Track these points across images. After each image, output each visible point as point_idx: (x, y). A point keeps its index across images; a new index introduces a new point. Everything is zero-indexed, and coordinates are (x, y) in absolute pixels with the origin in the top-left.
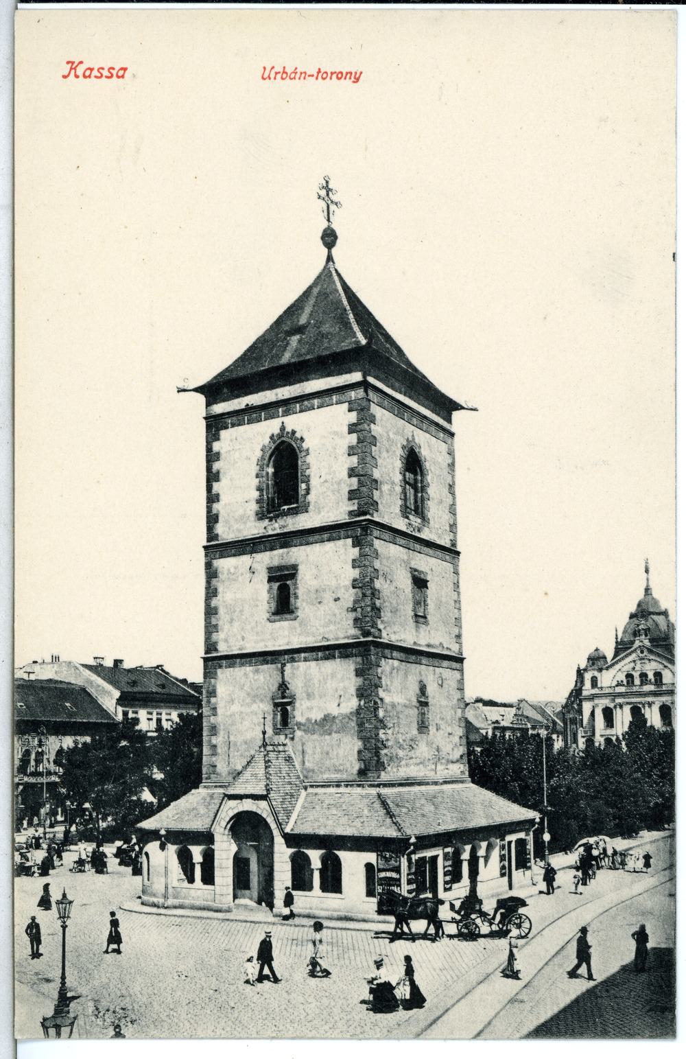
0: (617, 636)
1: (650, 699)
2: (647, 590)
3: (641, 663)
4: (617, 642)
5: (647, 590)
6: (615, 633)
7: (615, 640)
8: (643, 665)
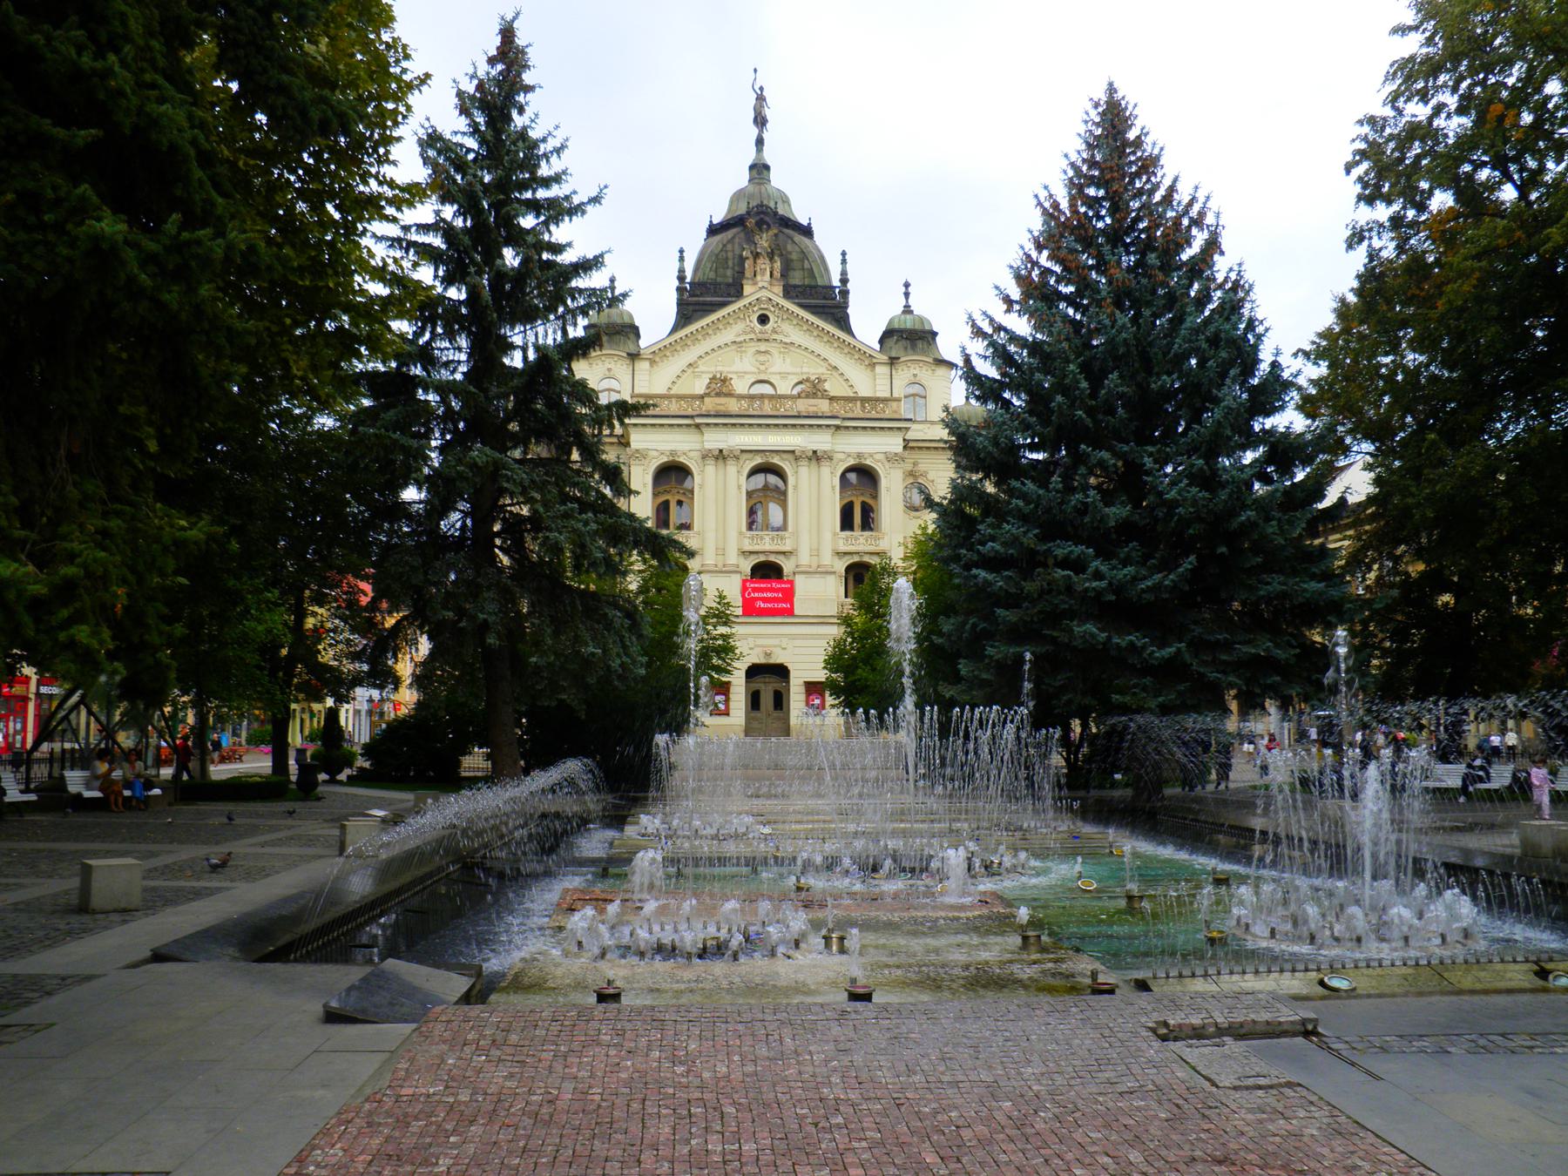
0: (682, 271)
1: (819, 441)
2: (759, 170)
3: (759, 352)
4: (680, 290)
5: (759, 170)
6: (677, 265)
7: (676, 283)
8: (762, 358)
